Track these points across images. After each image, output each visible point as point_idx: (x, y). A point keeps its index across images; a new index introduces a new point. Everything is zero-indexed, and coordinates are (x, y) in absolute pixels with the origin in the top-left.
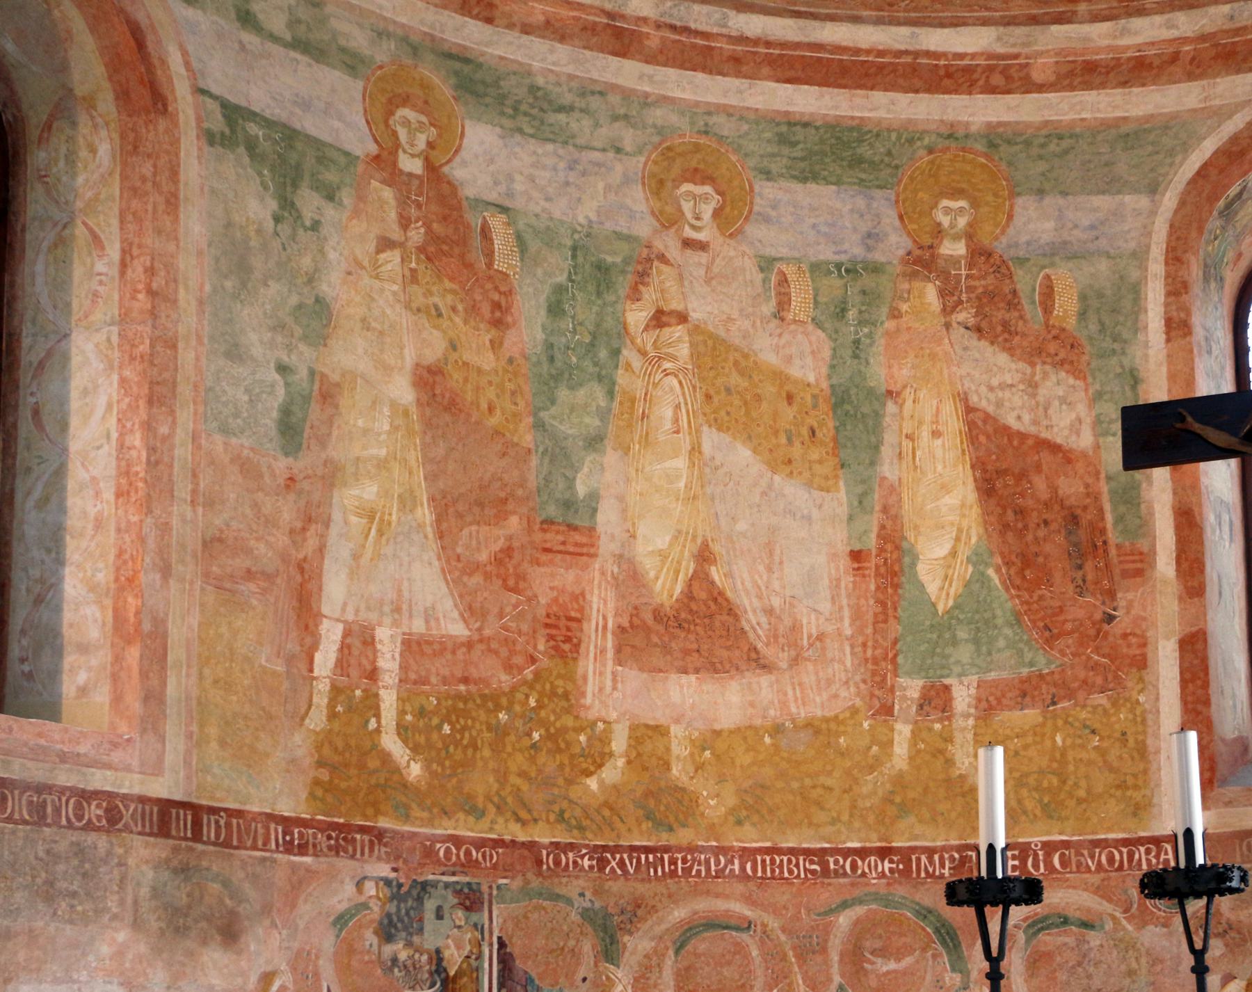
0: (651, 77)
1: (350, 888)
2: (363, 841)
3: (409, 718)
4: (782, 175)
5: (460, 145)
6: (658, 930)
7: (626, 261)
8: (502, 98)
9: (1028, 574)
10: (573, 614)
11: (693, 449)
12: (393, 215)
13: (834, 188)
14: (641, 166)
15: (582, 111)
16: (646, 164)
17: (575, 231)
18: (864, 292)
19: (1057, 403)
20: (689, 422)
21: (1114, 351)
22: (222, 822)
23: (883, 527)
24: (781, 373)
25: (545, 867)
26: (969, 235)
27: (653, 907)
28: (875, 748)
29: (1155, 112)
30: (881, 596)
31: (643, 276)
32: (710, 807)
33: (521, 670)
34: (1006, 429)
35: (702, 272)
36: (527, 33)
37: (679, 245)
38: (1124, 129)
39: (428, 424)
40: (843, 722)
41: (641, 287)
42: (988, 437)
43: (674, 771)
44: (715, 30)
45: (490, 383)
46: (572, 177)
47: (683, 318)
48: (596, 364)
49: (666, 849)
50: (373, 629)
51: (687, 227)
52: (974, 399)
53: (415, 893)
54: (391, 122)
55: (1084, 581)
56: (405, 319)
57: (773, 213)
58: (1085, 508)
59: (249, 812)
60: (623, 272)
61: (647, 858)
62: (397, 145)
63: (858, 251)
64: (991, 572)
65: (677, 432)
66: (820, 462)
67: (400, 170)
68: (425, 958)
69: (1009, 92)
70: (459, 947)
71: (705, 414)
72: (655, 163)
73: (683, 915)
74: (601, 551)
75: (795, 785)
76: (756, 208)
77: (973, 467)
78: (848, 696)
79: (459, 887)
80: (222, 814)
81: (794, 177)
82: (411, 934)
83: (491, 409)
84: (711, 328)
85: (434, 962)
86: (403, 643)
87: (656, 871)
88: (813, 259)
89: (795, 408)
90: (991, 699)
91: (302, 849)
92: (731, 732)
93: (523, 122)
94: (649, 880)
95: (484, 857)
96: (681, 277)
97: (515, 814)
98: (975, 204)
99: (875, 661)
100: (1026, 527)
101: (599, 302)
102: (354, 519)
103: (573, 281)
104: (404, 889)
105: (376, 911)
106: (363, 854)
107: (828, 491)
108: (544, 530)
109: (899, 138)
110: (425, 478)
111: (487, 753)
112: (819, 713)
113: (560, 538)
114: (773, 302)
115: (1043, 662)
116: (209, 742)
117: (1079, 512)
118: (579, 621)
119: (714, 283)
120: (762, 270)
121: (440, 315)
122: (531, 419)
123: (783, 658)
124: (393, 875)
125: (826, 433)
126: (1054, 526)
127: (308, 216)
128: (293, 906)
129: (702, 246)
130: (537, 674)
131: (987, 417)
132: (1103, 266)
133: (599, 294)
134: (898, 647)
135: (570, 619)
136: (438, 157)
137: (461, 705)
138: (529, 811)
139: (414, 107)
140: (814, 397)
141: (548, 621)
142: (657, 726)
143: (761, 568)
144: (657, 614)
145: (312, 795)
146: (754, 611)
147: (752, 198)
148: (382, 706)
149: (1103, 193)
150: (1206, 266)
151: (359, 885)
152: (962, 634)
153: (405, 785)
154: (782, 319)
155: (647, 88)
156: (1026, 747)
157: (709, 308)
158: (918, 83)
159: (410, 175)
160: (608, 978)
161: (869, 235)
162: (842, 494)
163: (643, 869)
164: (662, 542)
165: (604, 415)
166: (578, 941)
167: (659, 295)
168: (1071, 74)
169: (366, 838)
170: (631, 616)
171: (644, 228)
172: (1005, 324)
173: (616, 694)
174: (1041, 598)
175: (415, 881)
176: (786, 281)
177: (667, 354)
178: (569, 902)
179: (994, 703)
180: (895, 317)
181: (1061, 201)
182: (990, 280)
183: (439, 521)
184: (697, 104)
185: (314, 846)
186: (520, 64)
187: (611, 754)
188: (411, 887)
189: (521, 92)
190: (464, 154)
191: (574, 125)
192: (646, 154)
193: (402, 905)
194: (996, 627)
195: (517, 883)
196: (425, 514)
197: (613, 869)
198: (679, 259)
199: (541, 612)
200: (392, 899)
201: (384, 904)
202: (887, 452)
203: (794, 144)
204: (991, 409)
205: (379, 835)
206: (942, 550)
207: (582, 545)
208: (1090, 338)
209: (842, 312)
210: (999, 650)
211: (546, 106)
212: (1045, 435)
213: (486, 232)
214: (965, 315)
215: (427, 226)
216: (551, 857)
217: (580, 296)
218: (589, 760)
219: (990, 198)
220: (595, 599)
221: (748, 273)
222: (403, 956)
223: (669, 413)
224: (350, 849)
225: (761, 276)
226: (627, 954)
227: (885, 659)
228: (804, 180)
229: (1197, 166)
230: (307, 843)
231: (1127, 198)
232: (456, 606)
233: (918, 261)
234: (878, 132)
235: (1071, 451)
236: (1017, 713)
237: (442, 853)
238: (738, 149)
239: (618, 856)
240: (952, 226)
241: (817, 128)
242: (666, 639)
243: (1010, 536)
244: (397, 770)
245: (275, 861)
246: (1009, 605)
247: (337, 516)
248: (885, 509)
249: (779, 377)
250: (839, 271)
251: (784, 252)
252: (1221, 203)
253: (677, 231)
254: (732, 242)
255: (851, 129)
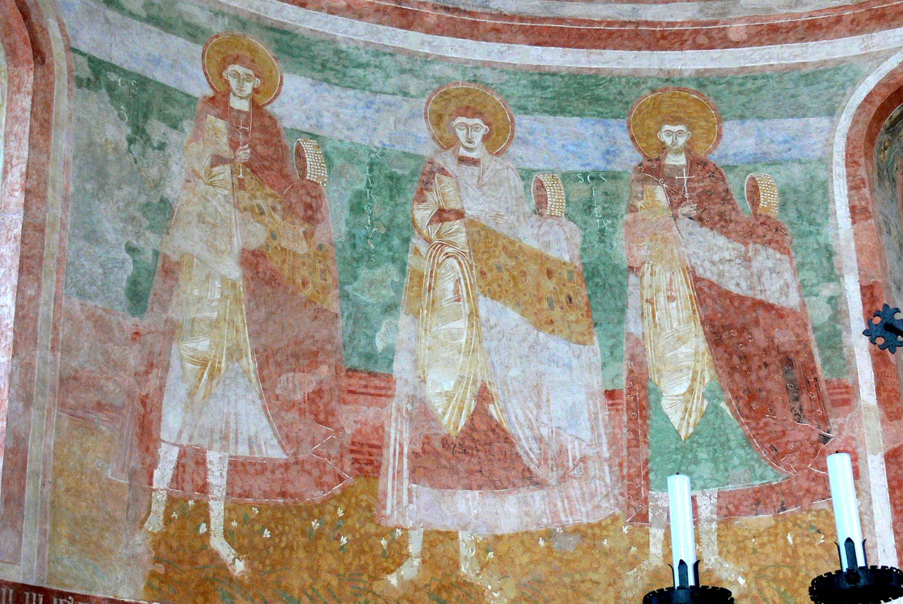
0: (430, 43)
3: (234, 524)
5: (280, 91)
7: (413, 174)
8: (313, 58)
9: (754, 405)
10: (375, 442)
11: (471, 313)
12: (225, 140)
13: (577, 119)
14: (424, 105)
15: (376, 67)
16: (427, 103)
17: (371, 152)
18: (606, 194)
19: (767, 272)
20: (468, 293)
21: (811, 233)
23: (631, 371)
24: (542, 255)
26: (688, 150)
28: (634, 549)
29: (827, 58)
30: (632, 426)
31: (426, 186)
32: (494, 598)
33: (330, 487)
34: (728, 293)
35: (475, 181)
36: (332, 14)
37: (456, 161)
38: (804, 71)
39: (252, 294)
40: (605, 528)
41: (425, 192)
42: (714, 300)
43: (463, 569)
44: (479, 10)
45: (304, 264)
46: (369, 113)
47: (460, 215)
48: (390, 249)
50: (205, 452)
51: (461, 149)
52: (700, 272)
54: (224, 74)
55: (801, 410)
56: (235, 216)
57: (531, 138)
58: (797, 352)
60: (410, 181)
62: (229, 90)
63: (600, 164)
64: (723, 405)
65: (459, 300)
66: (577, 322)
67: (232, 108)
69: (712, 47)
71: (481, 287)
72: (435, 102)
74: (397, 393)
75: (567, 580)
76: (516, 134)
77: (702, 323)
78: (609, 507)
81: (546, 112)
83: (304, 284)
84: (483, 222)
86: (230, 464)
88: (564, 171)
89: (554, 280)
90: (730, 506)
92: (510, 537)
93: (330, 75)
98: (691, 127)
99: (630, 477)
100: (750, 369)
101: (392, 203)
102: (189, 366)
103: (370, 188)
107: (585, 344)
108: (349, 377)
109: (628, 82)
110: (250, 335)
111: (301, 554)
112: (585, 521)
113: (363, 383)
114: (533, 202)
115: (771, 475)
116: (60, 539)
117: (792, 356)
118: (379, 447)
119: (485, 188)
120: (523, 179)
121: (262, 213)
122: (338, 291)
123: (552, 478)
125: (580, 300)
126: (773, 367)
127: (156, 139)
129: (475, 162)
130: (344, 490)
131: (712, 285)
132: (796, 169)
133: (392, 198)
134: (649, 465)
135: (372, 446)
136: (261, 100)
137: (279, 515)
139: (243, 64)
140: (570, 272)
141: (354, 448)
142: (447, 533)
143: (531, 405)
144: (445, 442)
146: (527, 439)
147: (513, 126)
148: (212, 514)
149: (792, 116)
150: (879, 168)
152: (703, 455)
153: (231, 580)
155: (427, 50)
156: (762, 545)
157: (481, 207)
158: (639, 43)
159: (239, 111)
161: (608, 152)
162: (596, 346)
164: (448, 385)
165: (397, 288)
167: (440, 197)
168: (759, 33)
170: (423, 444)
171: (428, 150)
172: (721, 215)
173: (411, 507)
174: (766, 424)
176: (543, 186)
177: (449, 242)
179: (733, 509)
180: (632, 211)
181: (760, 124)
182: (707, 182)
183: (261, 369)
184: (467, 61)
186: (327, 34)
187: (408, 555)
189: (328, 55)
190: (282, 97)
191: (370, 78)
192: (427, 97)
194: (730, 449)
196: (250, 363)
198: (455, 171)
199: (347, 441)
202: (631, 313)
203: (544, 88)
204: (714, 279)
206: (682, 388)
207: (381, 388)
208: (791, 223)
209: (588, 208)
210: (734, 467)
211: (347, 63)
212: (759, 297)
213: (299, 152)
214: (689, 209)
215: (253, 147)
217: (376, 199)
218: (390, 560)
219: (703, 123)
220: (393, 431)
221: (512, 182)
223: (451, 286)
225: (522, 183)
227: (639, 476)
228: (554, 114)
229: (864, 95)
231: (812, 120)
232: (275, 435)
233: (648, 170)
234: (612, 78)
235: (782, 308)
236: (753, 518)
238: (500, 93)
240: (674, 144)
241: (562, 77)
242: (453, 462)
243: (737, 376)
244: (224, 567)
246: (740, 430)
247: (175, 362)
248: (632, 358)
249: (540, 258)
250: (585, 179)
251: (541, 166)
252: (887, 122)
253: (454, 152)
254: (499, 159)
255: (590, 76)
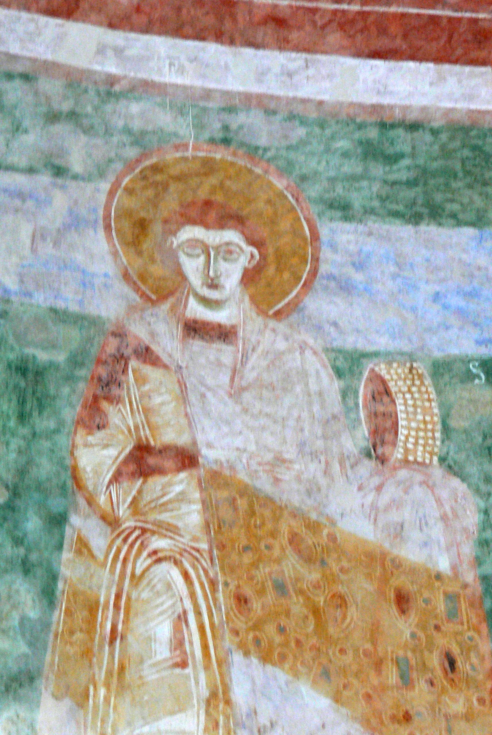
0: (119, 52)
4: (370, 211)
11: (214, 695)
13: (470, 231)
14: (103, 198)
16: (112, 193)
20: (205, 647)
24: (384, 555)
35: (226, 379)
37: (179, 331)
41: (105, 405)
48: (18, 542)
51: (192, 302)
57: (358, 277)
60: (70, 378)
65: (183, 665)
71: (237, 633)
72: (130, 191)
76: (324, 268)
81: (396, 214)
84: (242, 476)
88: (438, 355)
89: (413, 618)
96: (182, 385)
101: (25, 431)
119: (247, 396)
120: (339, 373)
140: (449, 597)
147: (317, 250)
154: (382, 460)
157: (238, 442)
167: (140, 418)
176: (387, 392)
177: (159, 524)
192: (112, 178)
198: (177, 355)
221: (312, 380)
225: (337, 385)
241: (435, 132)
253: (173, 309)
254: (281, 327)
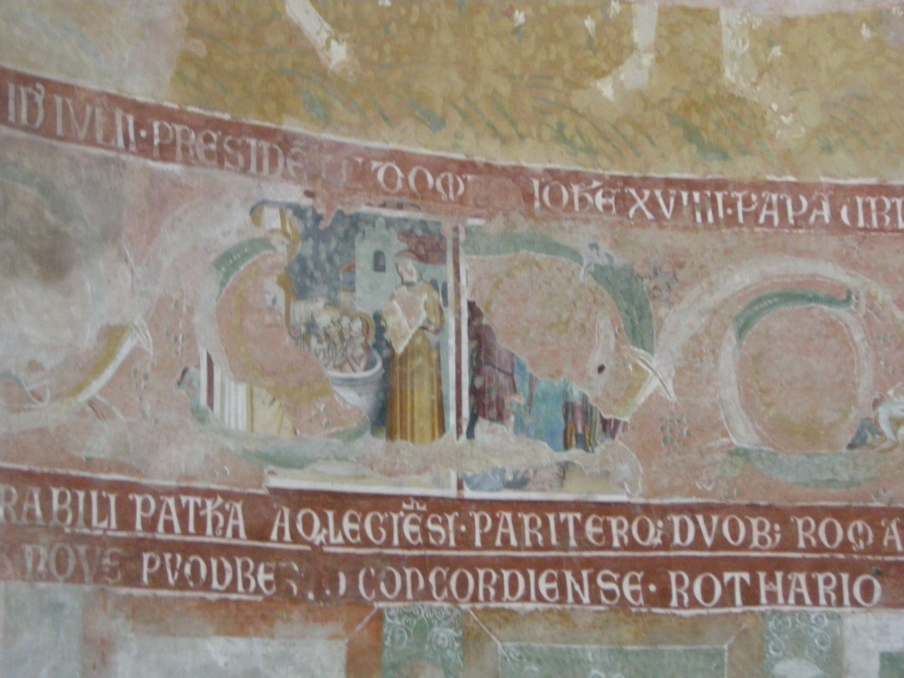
1: (240, 217)
2: (259, 150)
6: (710, 301)
22: (39, 99)
25: (537, 204)
27: (702, 267)
32: (783, 126)
43: (728, 74)
49: (720, 185)
53: (340, 230)
59: (83, 90)
61: (691, 198)
68: (358, 325)
70: (409, 311)
73: (748, 281)
79: (407, 227)
80: (39, 86)
82: (336, 290)
85: (372, 332)
87: (704, 217)
91: (166, 152)
92: (810, 21)
94: (695, 229)
95: (445, 186)
97: (490, 125)
104: (323, 225)
105: (281, 253)
106: (260, 167)
111: (446, 37)
124: (306, 202)
128: (153, 233)
138: (513, 123)
142: (700, 11)
145: (180, 75)
151: (256, 212)
153: (324, 75)
160: (636, 367)
163: (686, 212)
166: (589, 312)
169: (265, 145)
175: (340, 212)
178: (575, 255)
185: (185, 149)
187: (633, 48)
188: (335, 220)
193: (322, 247)
195: (497, 225)
197: (639, 211)
200: (305, 237)
201: (294, 243)
205: (286, 141)
216: (546, 190)
218: (601, 55)
222: (324, 320)
224: (241, 159)
226: (663, 336)
230: (174, 144)
237: (381, 176)
239: (647, 193)
244: (310, 51)
245: (124, 165)
